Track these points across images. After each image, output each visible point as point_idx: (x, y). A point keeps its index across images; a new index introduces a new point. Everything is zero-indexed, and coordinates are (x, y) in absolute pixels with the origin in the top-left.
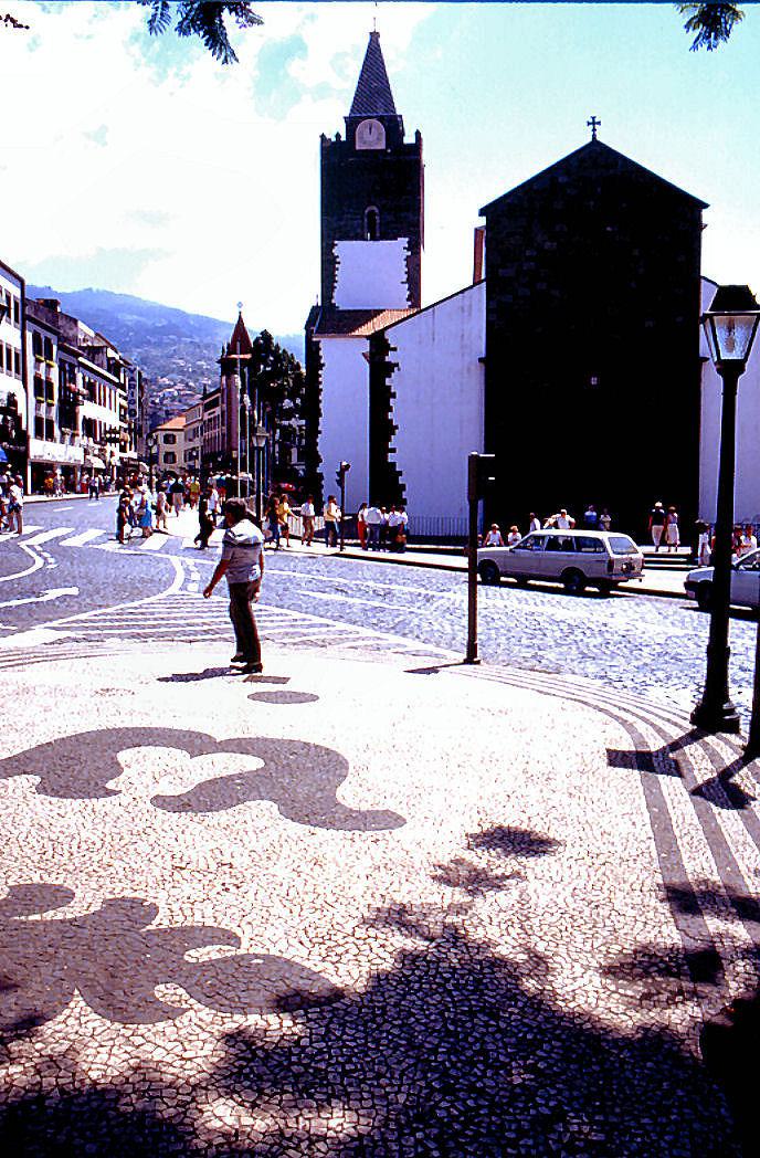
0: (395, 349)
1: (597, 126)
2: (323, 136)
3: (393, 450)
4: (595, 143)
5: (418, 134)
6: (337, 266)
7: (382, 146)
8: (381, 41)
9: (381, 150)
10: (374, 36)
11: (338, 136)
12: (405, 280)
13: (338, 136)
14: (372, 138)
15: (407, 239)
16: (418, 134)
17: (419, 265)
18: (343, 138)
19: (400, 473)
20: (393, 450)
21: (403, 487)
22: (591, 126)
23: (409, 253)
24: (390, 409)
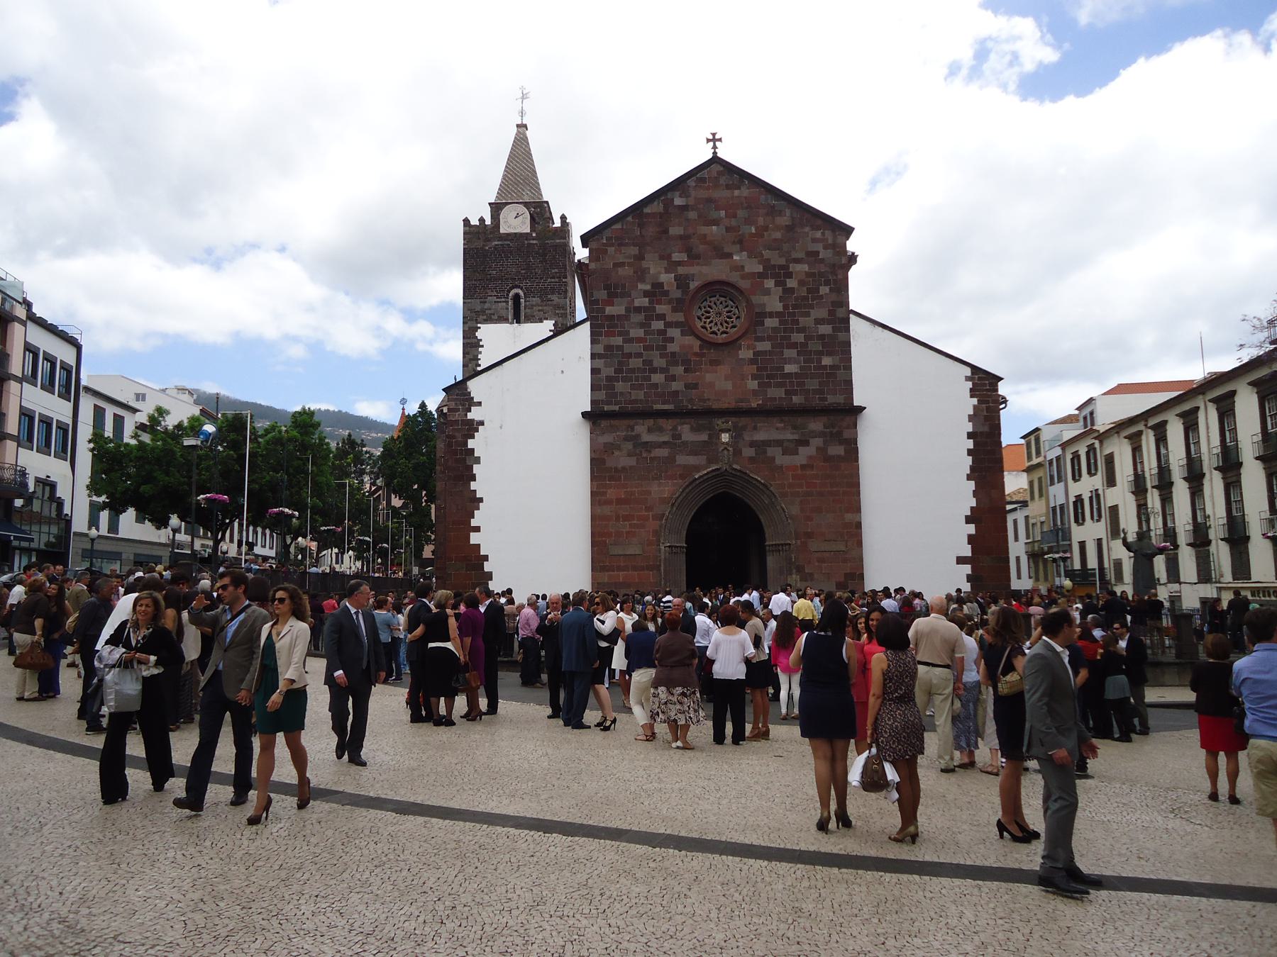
0: (479, 404)
1: (718, 144)
2: (466, 221)
3: (477, 529)
4: (715, 160)
5: (563, 218)
8: (528, 133)
10: (521, 127)
11: (482, 220)
13: (482, 220)
14: (516, 222)
16: (563, 218)
18: (488, 222)
19: (486, 558)
20: (477, 529)
21: (489, 576)
22: (711, 144)
24: (473, 478)
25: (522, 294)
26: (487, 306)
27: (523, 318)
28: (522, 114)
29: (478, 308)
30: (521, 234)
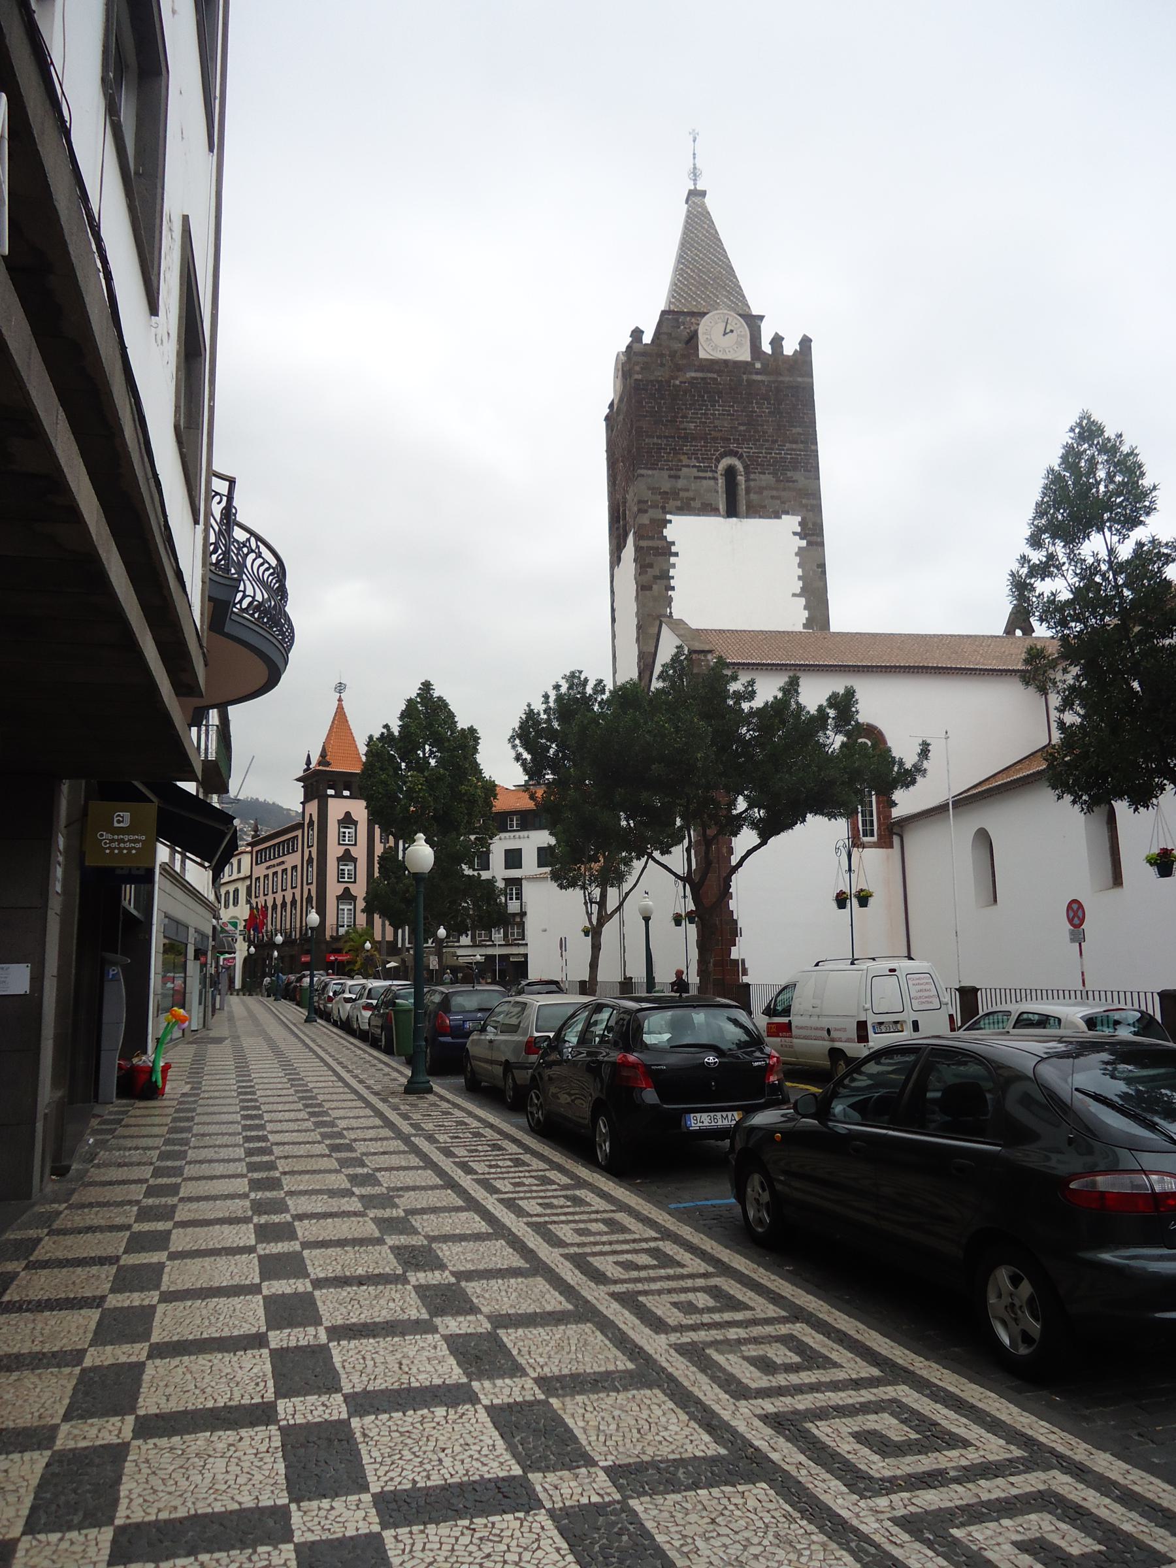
5: (806, 343)
6: (673, 560)
7: (745, 355)
9: (747, 362)
10: (695, 196)
12: (798, 591)
14: (718, 342)
15: (799, 519)
16: (806, 343)
17: (822, 566)
23: (804, 543)
25: (740, 466)
26: (680, 483)
27: (742, 507)
28: (695, 174)
29: (666, 486)
30: (736, 364)
